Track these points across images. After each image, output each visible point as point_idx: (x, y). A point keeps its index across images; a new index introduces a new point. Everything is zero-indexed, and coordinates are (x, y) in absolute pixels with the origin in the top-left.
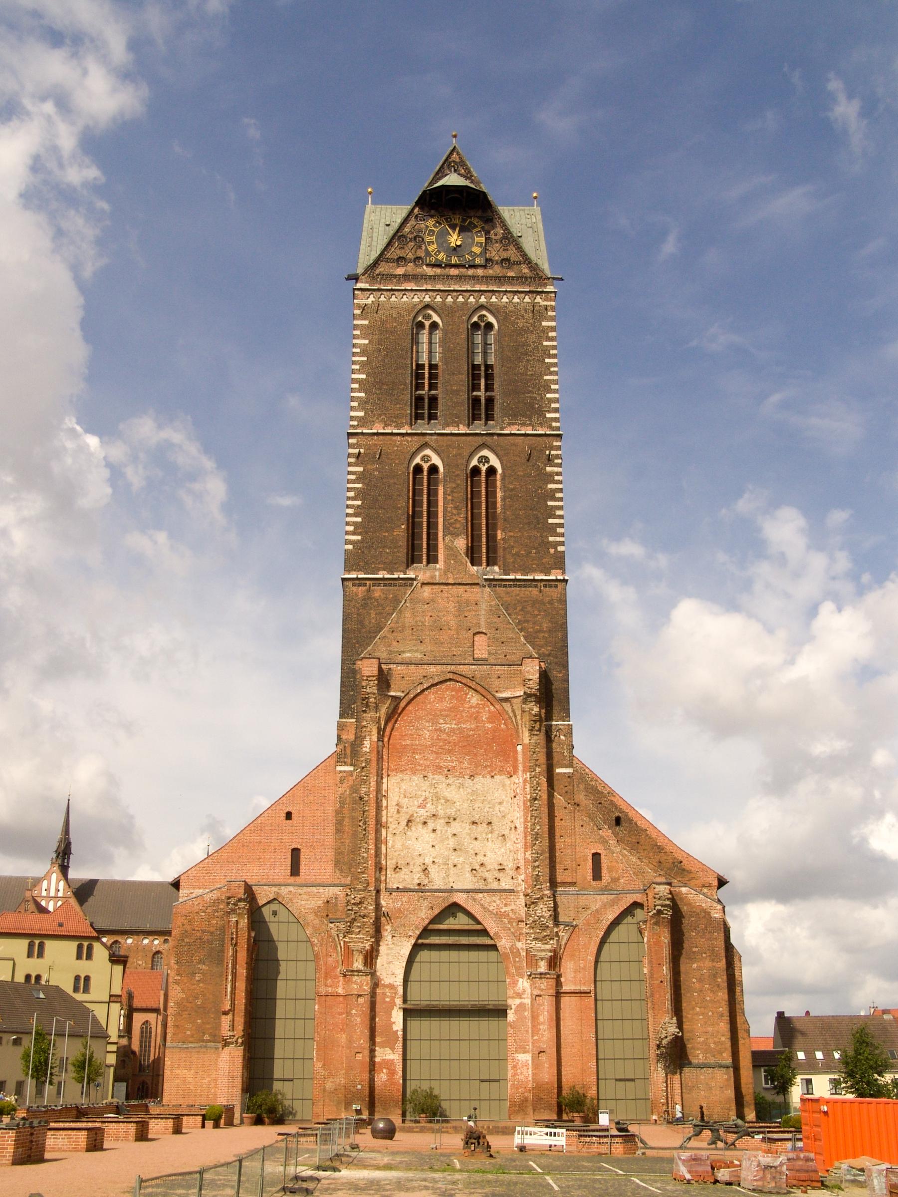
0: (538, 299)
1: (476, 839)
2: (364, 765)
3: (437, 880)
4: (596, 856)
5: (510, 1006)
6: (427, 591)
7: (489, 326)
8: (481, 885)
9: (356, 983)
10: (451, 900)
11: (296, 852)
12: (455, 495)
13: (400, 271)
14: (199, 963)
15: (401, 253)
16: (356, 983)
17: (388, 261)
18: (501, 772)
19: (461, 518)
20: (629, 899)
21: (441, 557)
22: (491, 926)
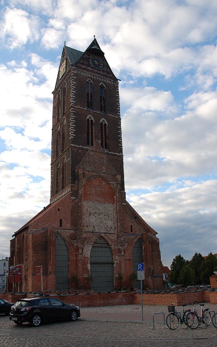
0: (115, 84)
1: (105, 220)
3: (97, 231)
4: (131, 226)
5: (114, 263)
6: (92, 153)
7: (104, 87)
8: (107, 232)
9: (80, 257)
10: (101, 235)
11: (61, 220)
12: (98, 129)
13: (83, 67)
14: (39, 250)
15: (83, 62)
16: (80, 257)
17: (80, 63)
18: (111, 203)
19: (100, 135)
20: (139, 237)
21: (94, 144)
22: (110, 243)
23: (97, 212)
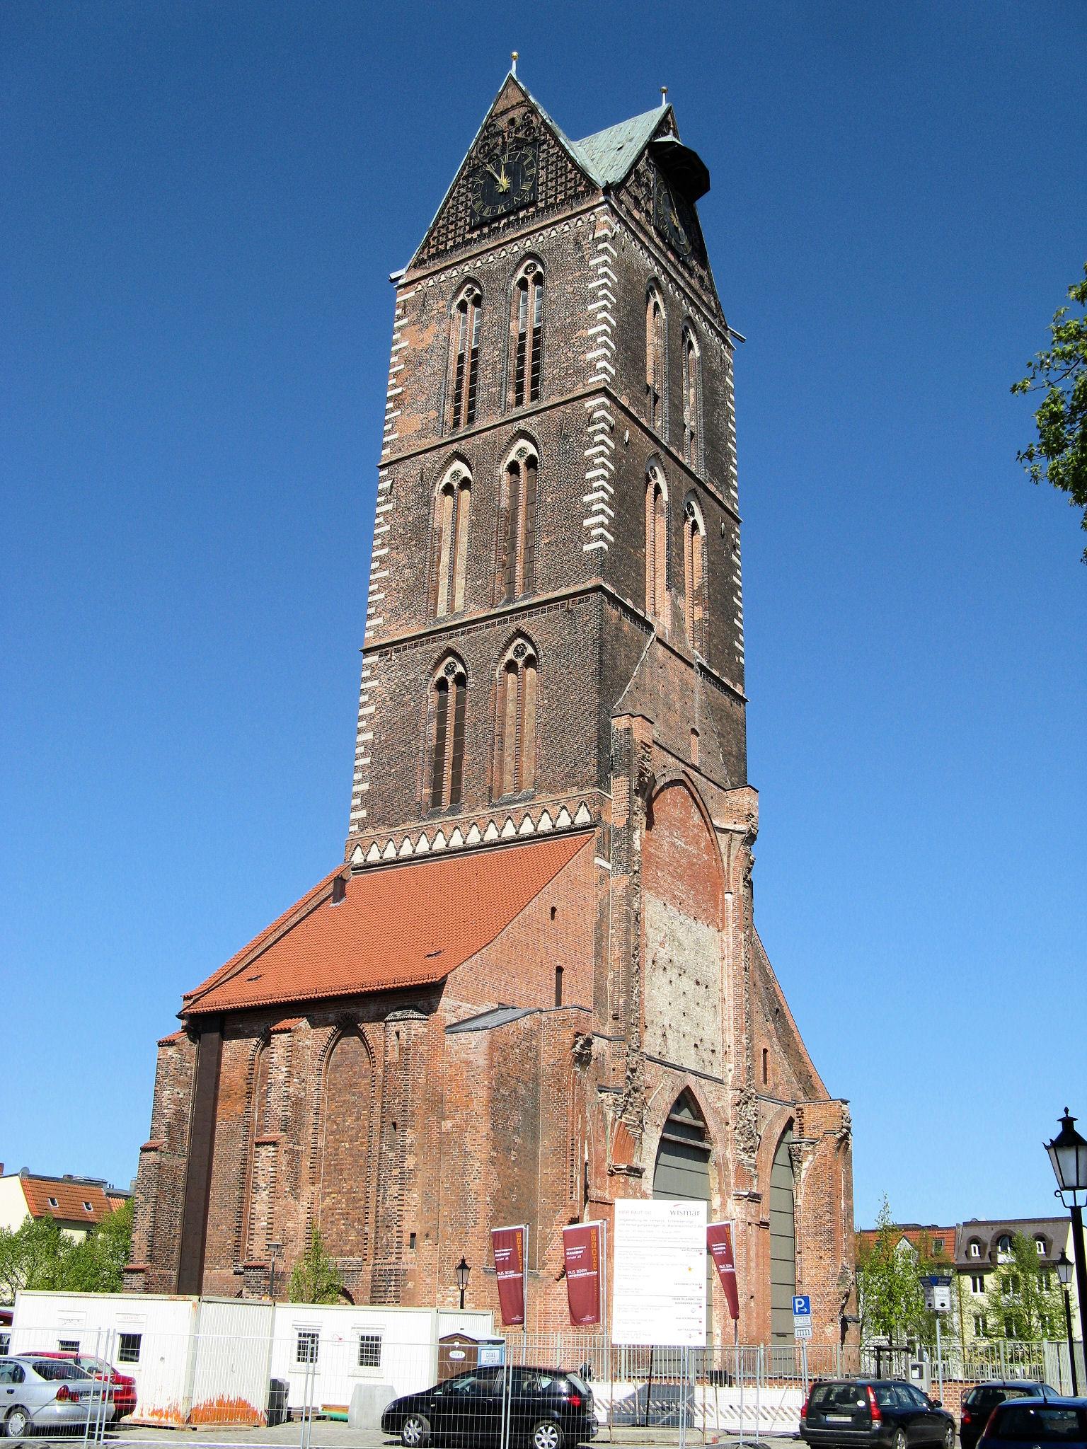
2: (636, 868)
23: (675, 959)
